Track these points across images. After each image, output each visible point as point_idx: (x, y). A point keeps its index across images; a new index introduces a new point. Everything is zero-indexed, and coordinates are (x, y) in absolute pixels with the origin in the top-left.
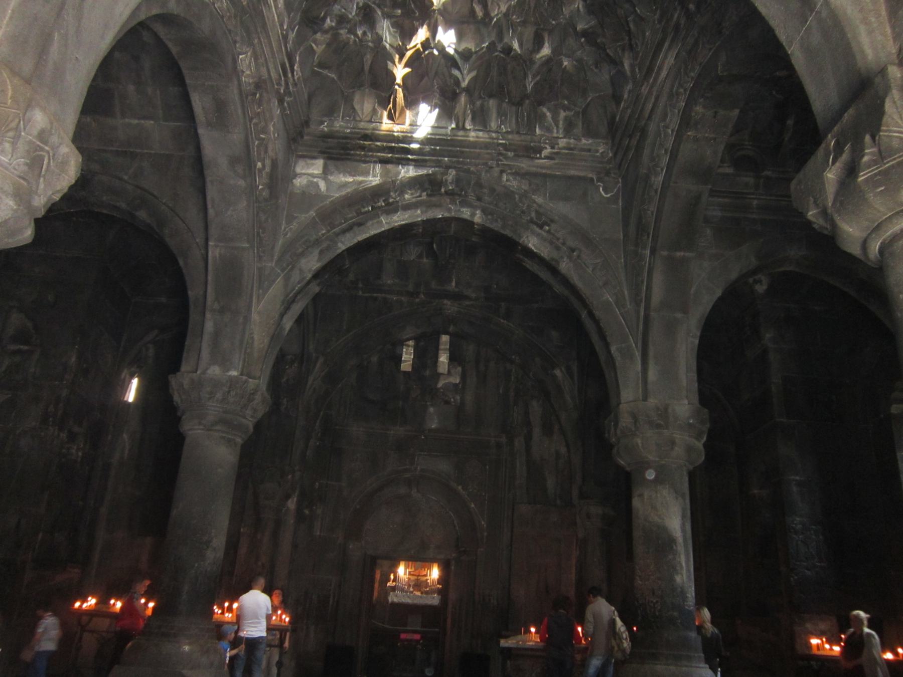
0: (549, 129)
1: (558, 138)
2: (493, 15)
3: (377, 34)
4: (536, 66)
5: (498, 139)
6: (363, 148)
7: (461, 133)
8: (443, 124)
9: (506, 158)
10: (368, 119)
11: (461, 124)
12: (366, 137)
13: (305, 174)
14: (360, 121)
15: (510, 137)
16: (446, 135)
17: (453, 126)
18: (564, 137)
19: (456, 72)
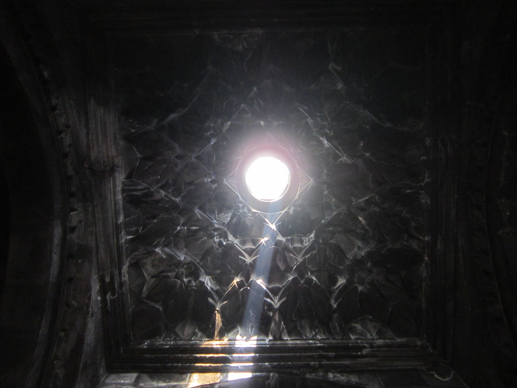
0: (362, 334)
1: (373, 339)
2: (292, 266)
3: (200, 281)
4: (335, 294)
5: (317, 344)
6: (179, 360)
7: (279, 342)
8: (261, 337)
9: (328, 358)
10: (188, 338)
11: (278, 336)
12: (185, 350)
13: (113, 384)
14: (181, 340)
15: (327, 341)
16: (265, 344)
17: (271, 338)
18: (380, 339)
19: (269, 300)
